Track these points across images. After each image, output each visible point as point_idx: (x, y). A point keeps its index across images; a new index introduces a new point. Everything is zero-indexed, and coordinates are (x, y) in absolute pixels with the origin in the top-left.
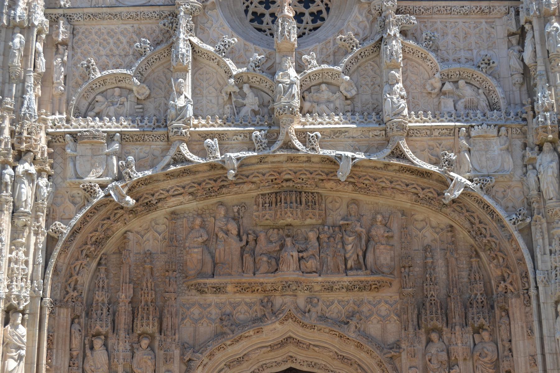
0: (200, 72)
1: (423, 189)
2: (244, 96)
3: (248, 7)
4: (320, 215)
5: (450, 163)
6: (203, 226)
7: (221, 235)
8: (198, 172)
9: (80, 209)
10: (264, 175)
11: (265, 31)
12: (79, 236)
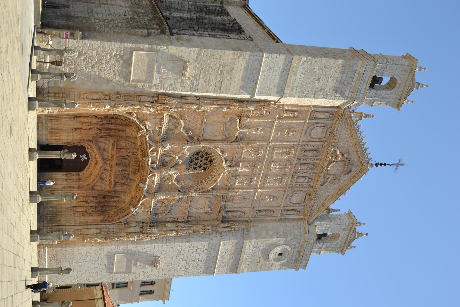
5: (141, 208)
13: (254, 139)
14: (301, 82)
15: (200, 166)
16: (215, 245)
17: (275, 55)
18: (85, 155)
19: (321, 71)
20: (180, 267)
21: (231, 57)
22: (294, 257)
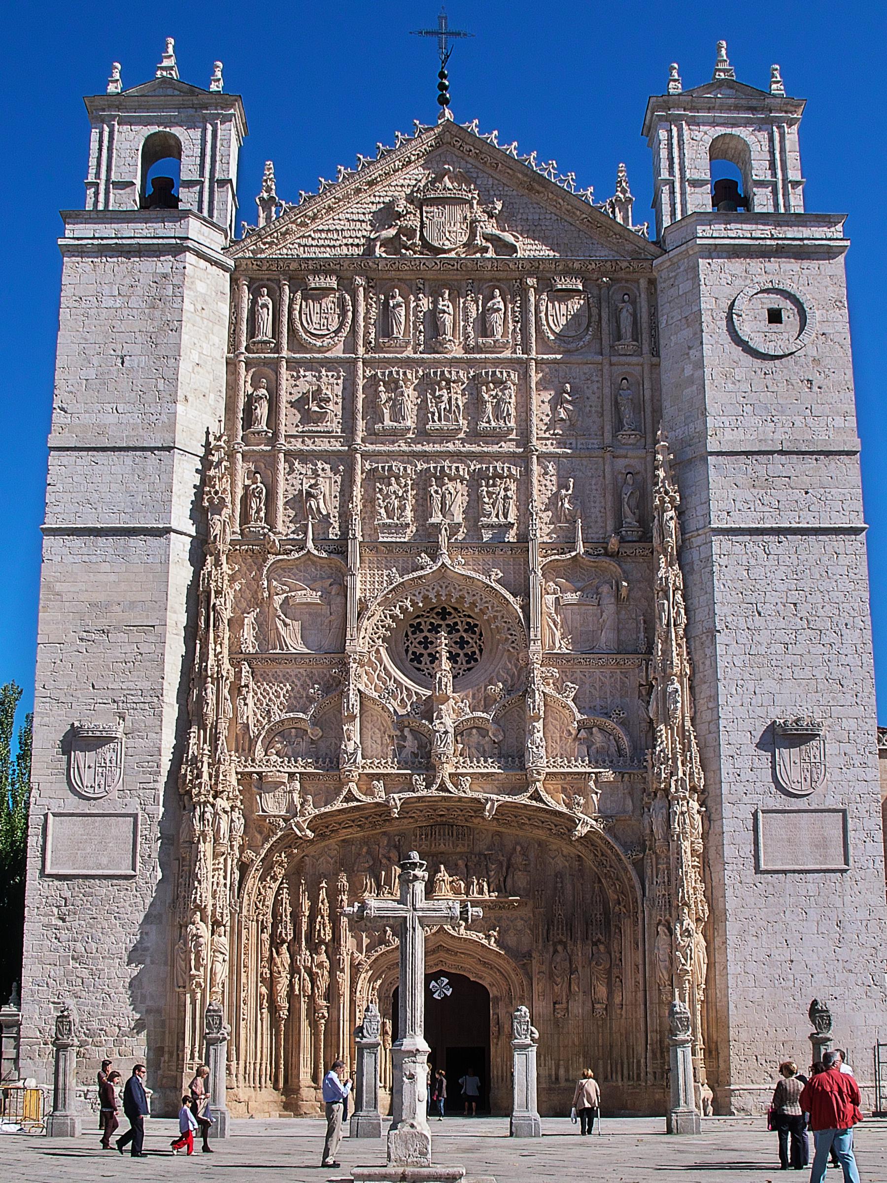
1: (556, 826)
2: (404, 738)
4: (468, 845)
7: (384, 861)
8: (366, 809)
9: (266, 840)
10: (421, 811)
11: (423, 671)
15: (462, 643)
20: (824, 650)
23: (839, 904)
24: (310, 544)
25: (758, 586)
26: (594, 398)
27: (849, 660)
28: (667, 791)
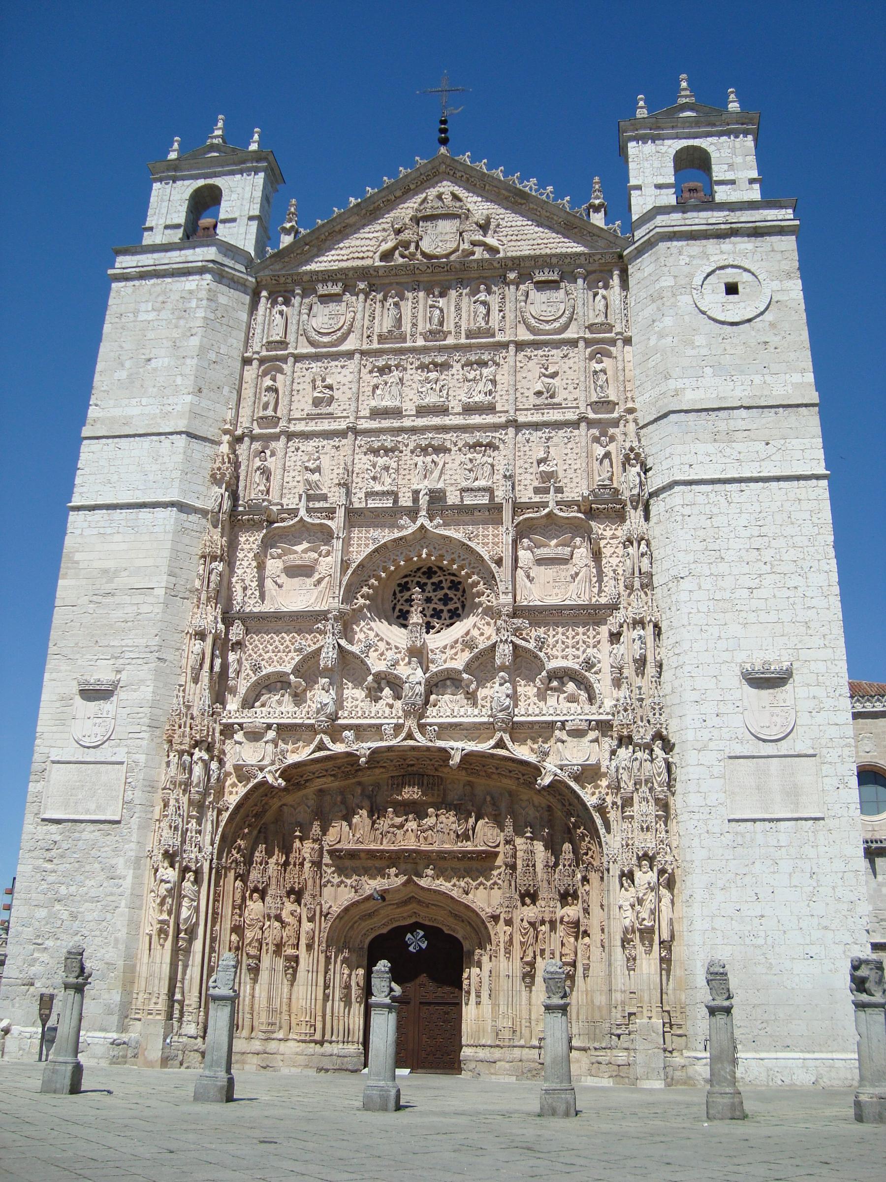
0: (348, 668)
1: (523, 775)
3: (395, 604)
4: (438, 795)
6: (343, 802)
8: (338, 758)
10: (392, 761)
12: (242, 810)
13: (341, 471)
14: (151, 400)
15: (446, 600)
16: (689, 497)
17: (78, 481)
18: (409, 936)
19: (128, 364)
20: (791, 593)
21: (73, 582)
22: (742, 246)
23: (812, 853)
24: (302, 513)
25: (721, 534)
26: (569, 372)
27: (814, 602)
28: (630, 738)
